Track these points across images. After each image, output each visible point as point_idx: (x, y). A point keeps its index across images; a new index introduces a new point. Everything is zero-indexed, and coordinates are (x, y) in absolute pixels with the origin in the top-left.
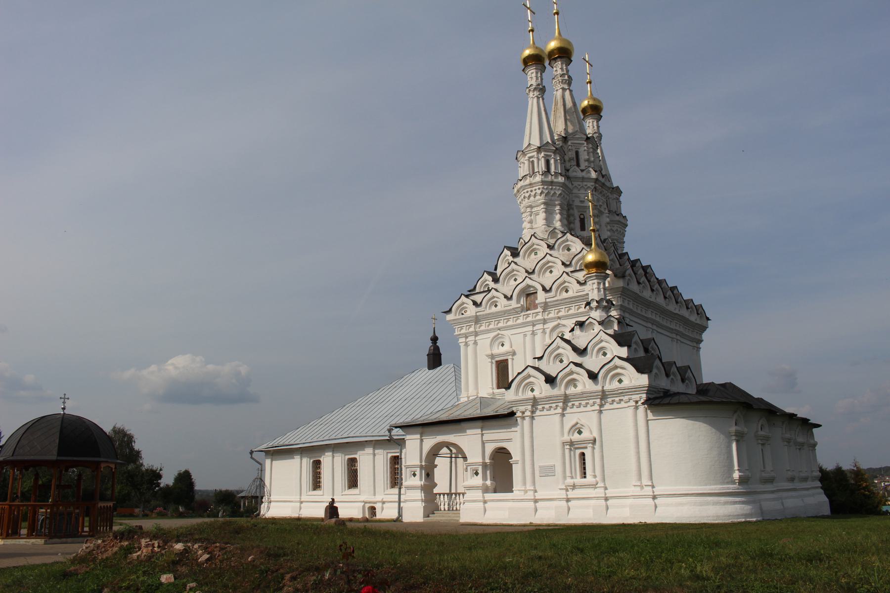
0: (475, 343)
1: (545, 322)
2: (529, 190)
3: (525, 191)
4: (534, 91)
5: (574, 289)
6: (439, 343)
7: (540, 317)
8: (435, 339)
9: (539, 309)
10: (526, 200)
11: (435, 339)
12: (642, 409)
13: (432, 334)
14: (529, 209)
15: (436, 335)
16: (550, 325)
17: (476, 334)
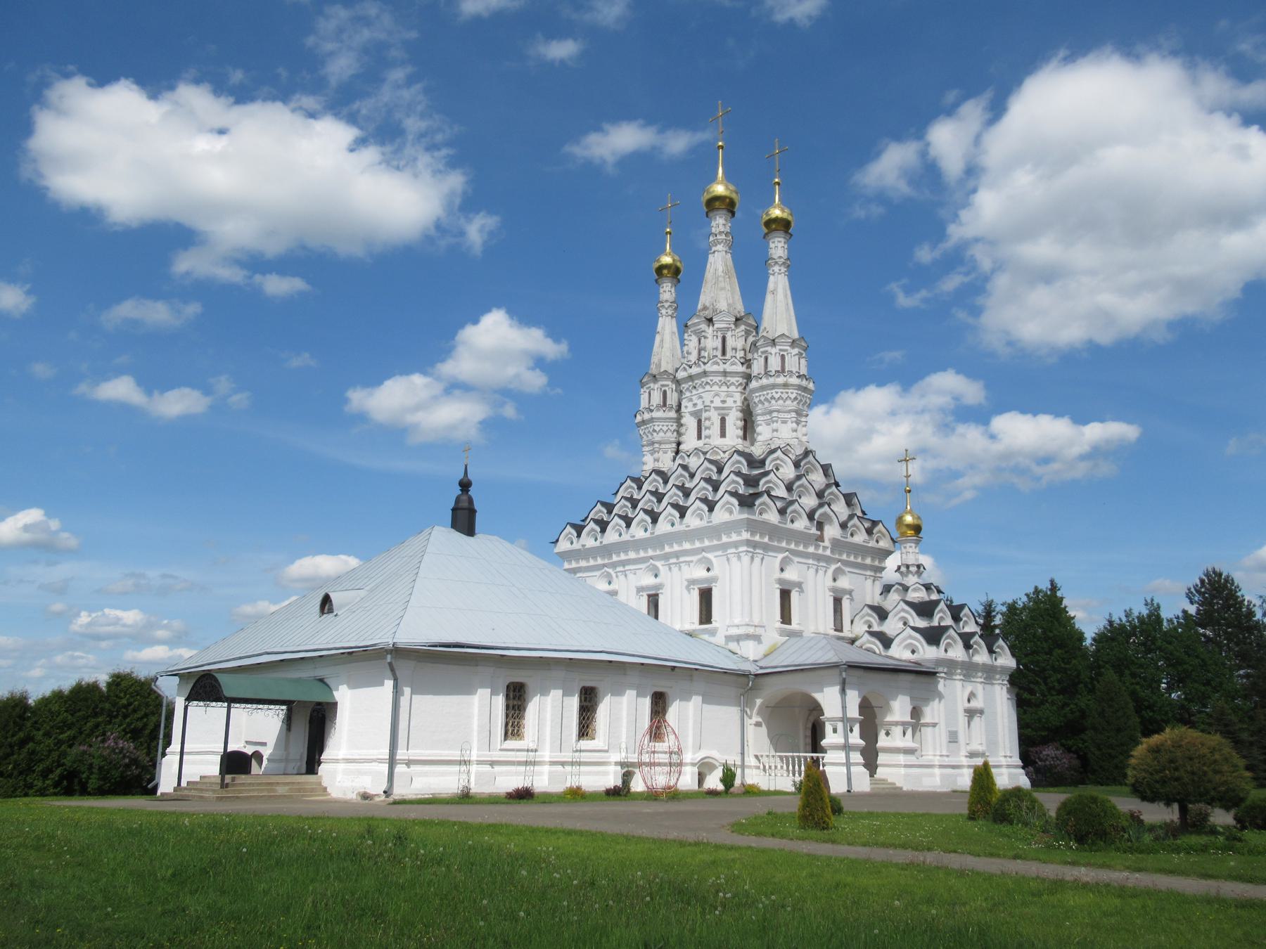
0: (762, 559)
1: (828, 560)
2: (803, 394)
3: (800, 392)
4: (780, 266)
5: (860, 538)
6: (472, 492)
7: (828, 553)
8: (465, 485)
9: (827, 543)
10: (795, 403)
11: (465, 485)
12: (1005, 688)
13: (461, 476)
14: (794, 414)
15: (470, 476)
16: (833, 567)
17: (766, 548)
